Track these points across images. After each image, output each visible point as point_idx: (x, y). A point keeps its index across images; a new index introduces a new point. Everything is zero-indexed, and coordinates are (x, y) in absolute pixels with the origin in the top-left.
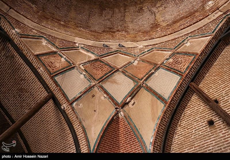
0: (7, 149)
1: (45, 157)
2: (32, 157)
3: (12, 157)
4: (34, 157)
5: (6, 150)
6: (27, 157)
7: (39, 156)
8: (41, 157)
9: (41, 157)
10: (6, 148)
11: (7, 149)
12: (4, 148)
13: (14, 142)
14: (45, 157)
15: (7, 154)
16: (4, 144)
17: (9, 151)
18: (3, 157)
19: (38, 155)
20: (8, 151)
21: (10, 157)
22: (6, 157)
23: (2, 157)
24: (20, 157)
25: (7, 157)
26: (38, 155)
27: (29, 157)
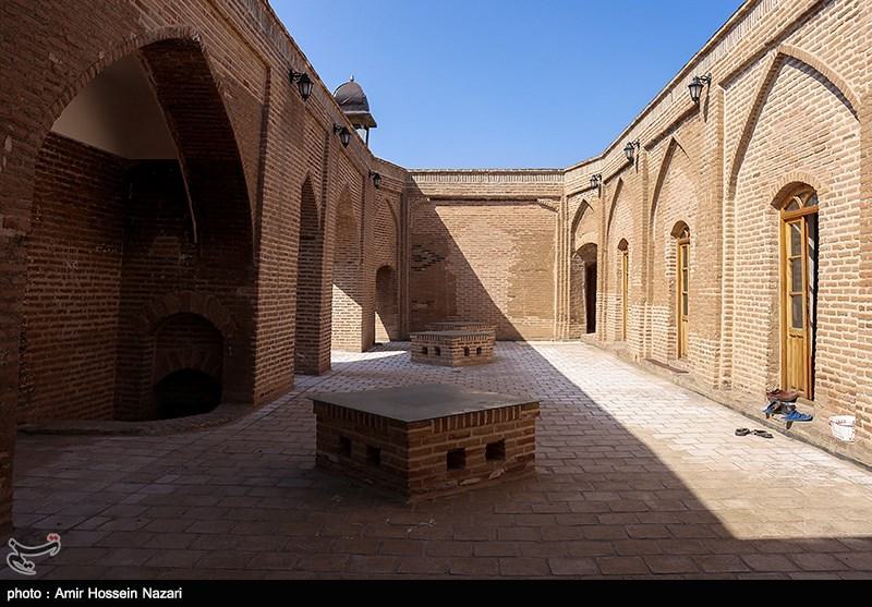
0: (26, 566)
1: (172, 594)
2: (123, 594)
3: (44, 595)
4: (130, 594)
5: (24, 568)
6: (102, 594)
7: (148, 593)
8: (156, 594)
9: (156, 594)
10: (22, 562)
11: (26, 566)
12: (15, 562)
13: (51, 538)
14: (172, 594)
15: (25, 584)
16: (17, 547)
17: (35, 573)
18: (12, 594)
19: (145, 590)
20: (31, 572)
21: (38, 594)
22: (22, 595)
23: (9, 597)
24: (77, 594)
25: (26, 594)
26: (145, 590)
27: (108, 594)
